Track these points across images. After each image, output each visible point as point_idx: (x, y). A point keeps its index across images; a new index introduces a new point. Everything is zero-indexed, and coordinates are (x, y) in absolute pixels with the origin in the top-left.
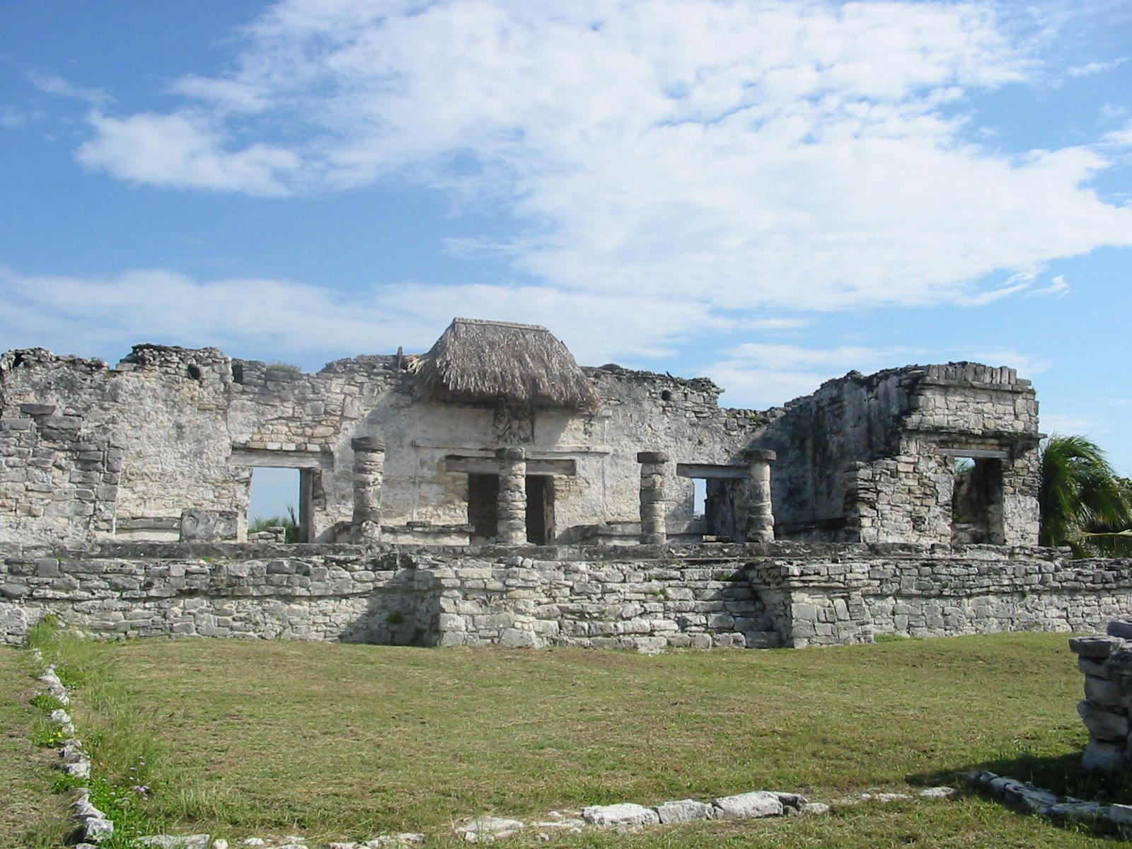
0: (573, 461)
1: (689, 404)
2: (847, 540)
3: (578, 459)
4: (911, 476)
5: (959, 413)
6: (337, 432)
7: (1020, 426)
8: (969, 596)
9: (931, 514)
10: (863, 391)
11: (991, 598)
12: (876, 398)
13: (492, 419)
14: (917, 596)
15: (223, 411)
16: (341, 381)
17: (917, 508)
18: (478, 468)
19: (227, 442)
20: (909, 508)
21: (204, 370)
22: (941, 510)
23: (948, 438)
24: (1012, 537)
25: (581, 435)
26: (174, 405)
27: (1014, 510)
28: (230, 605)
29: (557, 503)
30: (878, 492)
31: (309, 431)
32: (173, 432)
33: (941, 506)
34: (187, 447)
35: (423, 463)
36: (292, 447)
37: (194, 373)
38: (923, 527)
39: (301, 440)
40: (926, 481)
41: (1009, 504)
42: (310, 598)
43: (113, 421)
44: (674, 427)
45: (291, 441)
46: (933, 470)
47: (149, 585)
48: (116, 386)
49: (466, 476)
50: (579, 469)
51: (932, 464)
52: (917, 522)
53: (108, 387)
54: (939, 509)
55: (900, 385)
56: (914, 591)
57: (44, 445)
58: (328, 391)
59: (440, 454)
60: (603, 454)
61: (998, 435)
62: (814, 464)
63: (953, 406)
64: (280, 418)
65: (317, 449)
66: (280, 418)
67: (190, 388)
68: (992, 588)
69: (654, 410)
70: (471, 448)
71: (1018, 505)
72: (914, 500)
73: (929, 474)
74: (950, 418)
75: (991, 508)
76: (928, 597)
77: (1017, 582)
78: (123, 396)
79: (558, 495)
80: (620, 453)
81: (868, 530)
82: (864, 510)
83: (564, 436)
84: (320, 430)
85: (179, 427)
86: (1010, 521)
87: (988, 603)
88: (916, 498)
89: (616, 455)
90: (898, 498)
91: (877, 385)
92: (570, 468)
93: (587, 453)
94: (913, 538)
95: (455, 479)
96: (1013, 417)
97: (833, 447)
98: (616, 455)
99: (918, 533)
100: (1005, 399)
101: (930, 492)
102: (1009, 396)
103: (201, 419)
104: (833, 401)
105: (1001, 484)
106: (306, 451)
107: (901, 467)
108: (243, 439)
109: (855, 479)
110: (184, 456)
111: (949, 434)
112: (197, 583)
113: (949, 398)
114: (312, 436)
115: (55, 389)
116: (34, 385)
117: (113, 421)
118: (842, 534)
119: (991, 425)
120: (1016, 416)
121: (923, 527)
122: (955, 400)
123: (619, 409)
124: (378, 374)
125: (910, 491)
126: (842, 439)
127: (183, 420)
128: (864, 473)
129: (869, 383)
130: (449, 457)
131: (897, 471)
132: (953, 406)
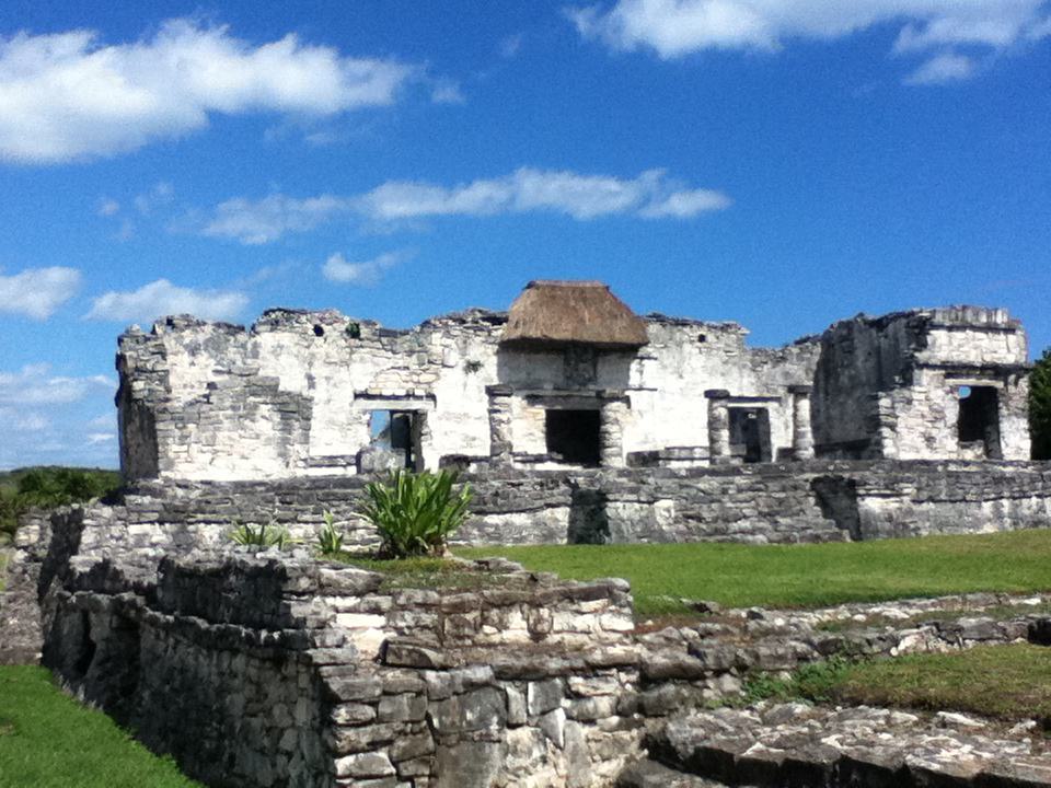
2: (870, 458)
7: (1010, 359)
9: (941, 435)
10: (874, 331)
12: (886, 337)
14: (945, 501)
15: (346, 363)
20: (923, 430)
23: (952, 370)
24: (1008, 452)
39: (411, 385)
40: (935, 407)
41: (1005, 426)
48: (256, 345)
52: (929, 440)
53: (249, 346)
54: (948, 431)
55: (907, 326)
62: (827, 393)
64: (393, 368)
75: (989, 429)
76: (955, 502)
81: (889, 449)
82: (886, 431)
90: (912, 422)
91: (887, 325)
94: (926, 455)
95: (535, 414)
97: (844, 380)
101: (938, 416)
104: (843, 339)
105: (997, 409)
107: (915, 396)
109: (878, 407)
115: (205, 350)
116: (186, 347)
118: (865, 453)
119: (988, 358)
121: (935, 445)
122: (958, 335)
123: (664, 351)
125: (923, 416)
126: (853, 372)
127: (313, 372)
128: (884, 402)
129: (879, 324)
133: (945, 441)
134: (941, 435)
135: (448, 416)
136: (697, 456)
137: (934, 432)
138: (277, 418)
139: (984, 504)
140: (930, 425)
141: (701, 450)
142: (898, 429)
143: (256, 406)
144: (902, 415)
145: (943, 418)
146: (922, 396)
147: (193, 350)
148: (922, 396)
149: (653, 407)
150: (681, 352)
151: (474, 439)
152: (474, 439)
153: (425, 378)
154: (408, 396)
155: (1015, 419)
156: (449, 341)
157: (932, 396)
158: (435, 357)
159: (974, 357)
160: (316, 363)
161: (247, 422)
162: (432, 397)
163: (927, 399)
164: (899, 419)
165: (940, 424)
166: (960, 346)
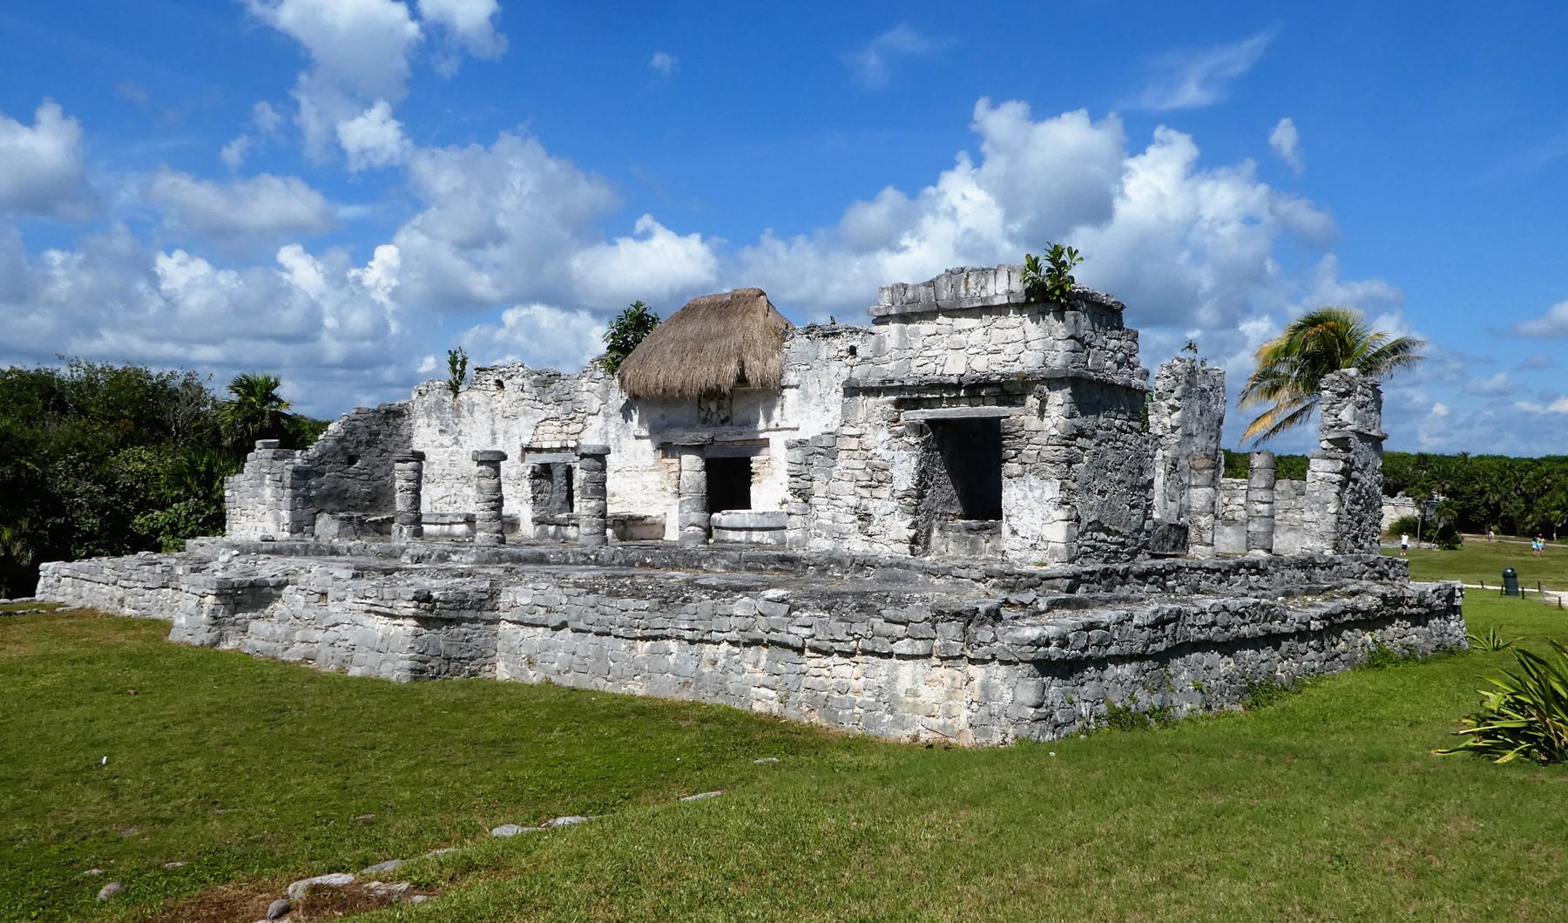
4: (856, 455)
11: (672, 645)
17: (864, 502)
20: (853, 501)
21: (506, 383)
27: (1020, 502)
29: (753, 489)
37: (500, 384)
38: (871, 529)
39: (564, 436)
40: (876, 461)
46: (885, 445)
64: (546, 419)
66: (546, 419)
71: (1029, 494)
72: (858, 490)
79: (754, 479)
86: (1013, 521)
88: (862, 487)
94: (857, 545)
99: (866, 538)
108: (526, 441)
121: (871, 529)
137: (872, 505)
140: (865, 493)
148: (854, 444)
153: (574, 427)
155: (1033, 480)
157: (869, 441)
159: (954, 367)
160: (497, 420)
165: (884, 492)
166: (927, 347)
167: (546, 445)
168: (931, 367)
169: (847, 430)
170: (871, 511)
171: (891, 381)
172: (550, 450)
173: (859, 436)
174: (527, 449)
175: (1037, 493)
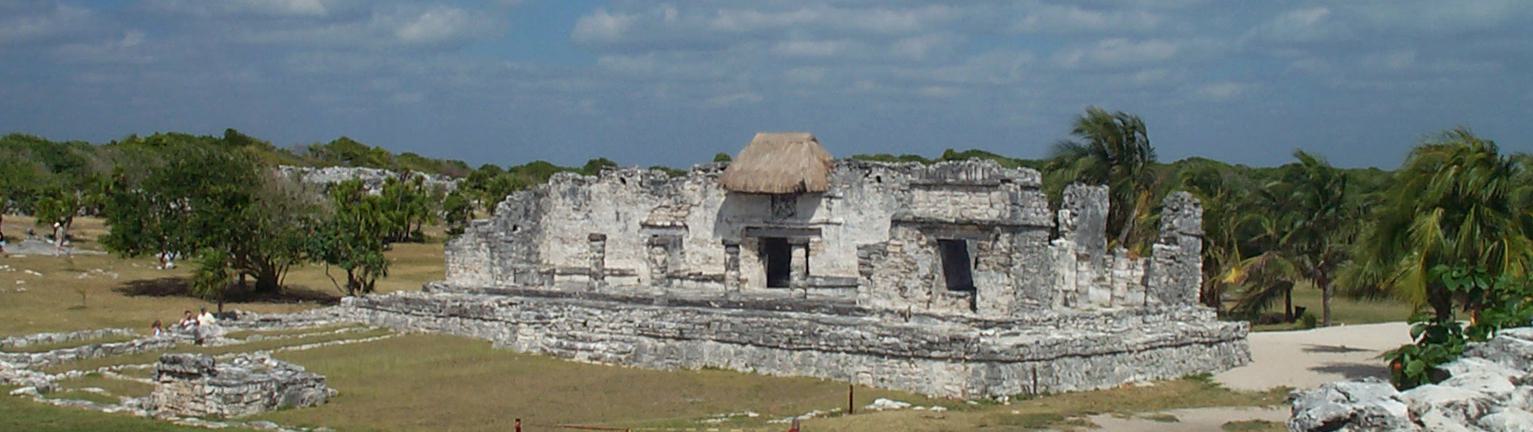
0: (820, 230)
1: (897, 185)
3: (823, 227)
5: (939, 205)
6: (689, 213)
7: (994, 214)
8: (799, 350)
13: (770, 202)
16: (689, 182)
18: (768, 234)
19: (638, 221)
20: (896, 279)
21: (627, 179)
22: (922, 282)
25: (825, 211)
26: (616, 202)
28: (465, 321)
30: (872, 267)
31: (674, 214)
32: (615, 216)
33: (922, 279)
34: (621, 224)
35: (733, 232)
36: (668, 224)
38: (906, 294)
39: (672, 219)
40: (909, 259)
42: (491, 320)
43: (590, 211)
44: (886, 203)
45: (667, 220)
47: (440, 311)
48: (590, 192)
49: (757, 240)
50: (824, 235)
51: (914, 246)
56: (761, 342)
57: (478, 240)
58: (683, 188)
59: (742, 226)
60: (839, 224)
61: (970, 222)
63: (933, 200)
65: (680, 224)
67: (622, 189)
68: (813, 346)
69: (872, 190)
70: (757, 222)
73: (912, 254)
74: (932, 210)
77: (832, 344)
78: (593, 198)
80: (849, 222)
83: (817, 212)
84: (680, 213)
85: (618, 213)
87: (811, 356)
89: (846, 225)
92: (819, 232)
93: (828, 223)
96: (988, 206)
98: (846, 225)
100: (981, 191)
102: (985, 189)
103: (626, 209)
106: (675, 226)
108: (644, 220)
110: (620, 231)
111: (931, 223)
112: (456, 311)
113: (930, 193)
114: (676, 217)
116: (561, 193)
117: (590, 211)
119: (967, 214)
120: (992, 206)
121: (906, 294)
123: (848, 191)
124: (708, 176)
127: (619, 210)
130: (748, 228)
131: (888, 253)
132: (933, 200)
133: (915, 291)
134: (913, 285)
135: (695, 241)
136: (818, 284)
138: (488, 250)
139: (796, 353)
141: (822, 280)
142: (872, 277)
143: (479, 244)
144: (878, 266)
145: (917, 270)
146: (898, 249)
147: (564, 197)
148: (898, 249)
149: (838, 238)
150: (861, 193)
151: (710, 258)
152: (710, 258)
154: (673, 226)
156: (696, 186)
157: (905, 249)
158: (685, 198)
161: (477, 253)
162: (686, 227)
163: (902, 252)
164: (875, 269)
165: (914, 275)
167: (659, 223)
168: (941, 212)
169: (893, 242)
170: (906, 285)
171: (919, 218)
172: (663, 227)
173: (901, 245)
174: (644, 225)
175: (995, 280)
